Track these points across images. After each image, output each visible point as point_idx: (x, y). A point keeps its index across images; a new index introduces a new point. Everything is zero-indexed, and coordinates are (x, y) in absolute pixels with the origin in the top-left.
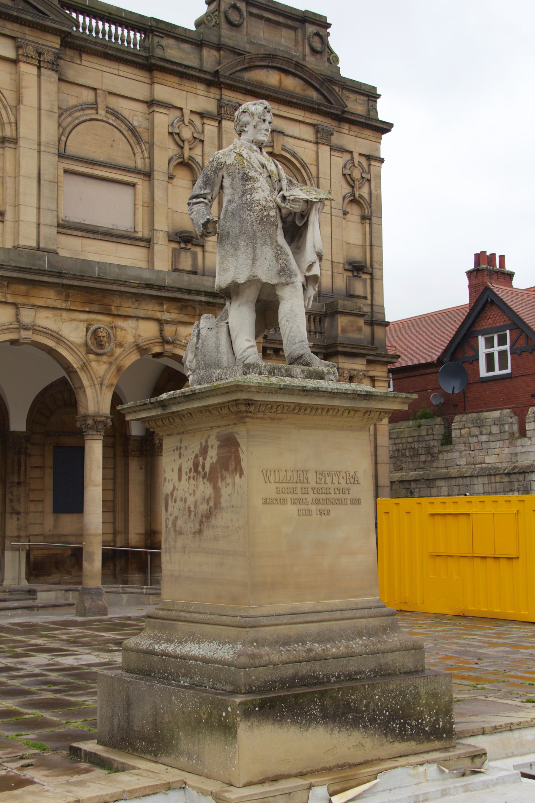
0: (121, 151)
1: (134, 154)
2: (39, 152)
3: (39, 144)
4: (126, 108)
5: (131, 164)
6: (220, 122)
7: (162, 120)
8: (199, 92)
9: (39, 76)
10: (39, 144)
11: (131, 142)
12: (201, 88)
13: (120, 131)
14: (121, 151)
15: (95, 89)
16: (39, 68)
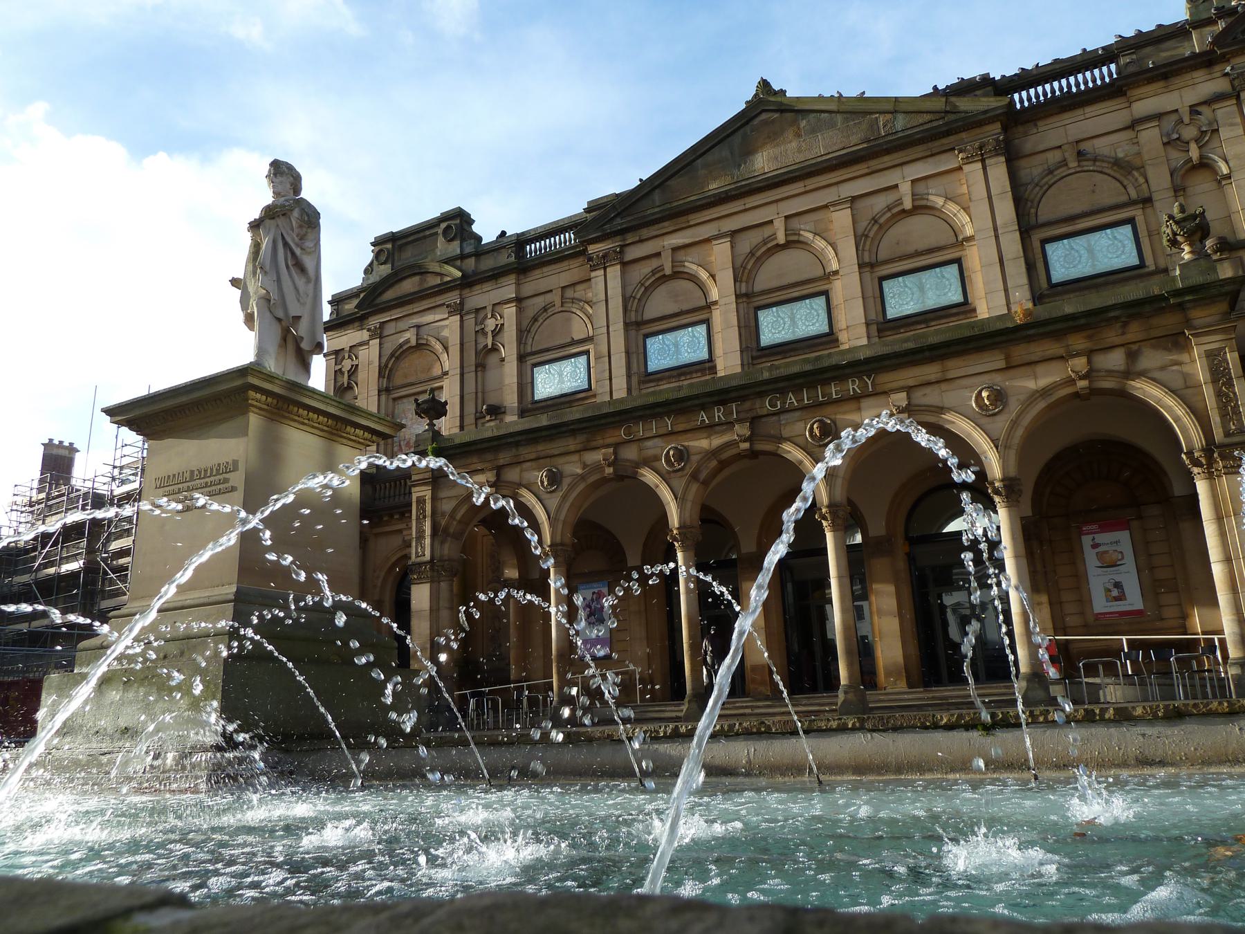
0: (1109, 191)
1: (1125, 187)
2: (997, 237)
3: (995, 230)
4: (1102, 146)
5: (1124, 198)
6: (1238, 97)
7: (1150, 136)
8: (1196, 81)
9: (984, 168)
10: (995, 230)
11: (1118, 176)
12: (1199, 75)
13: (1101, 172)
14: (1109, 191)
15: (1060, 147)
16: (983, 161)
